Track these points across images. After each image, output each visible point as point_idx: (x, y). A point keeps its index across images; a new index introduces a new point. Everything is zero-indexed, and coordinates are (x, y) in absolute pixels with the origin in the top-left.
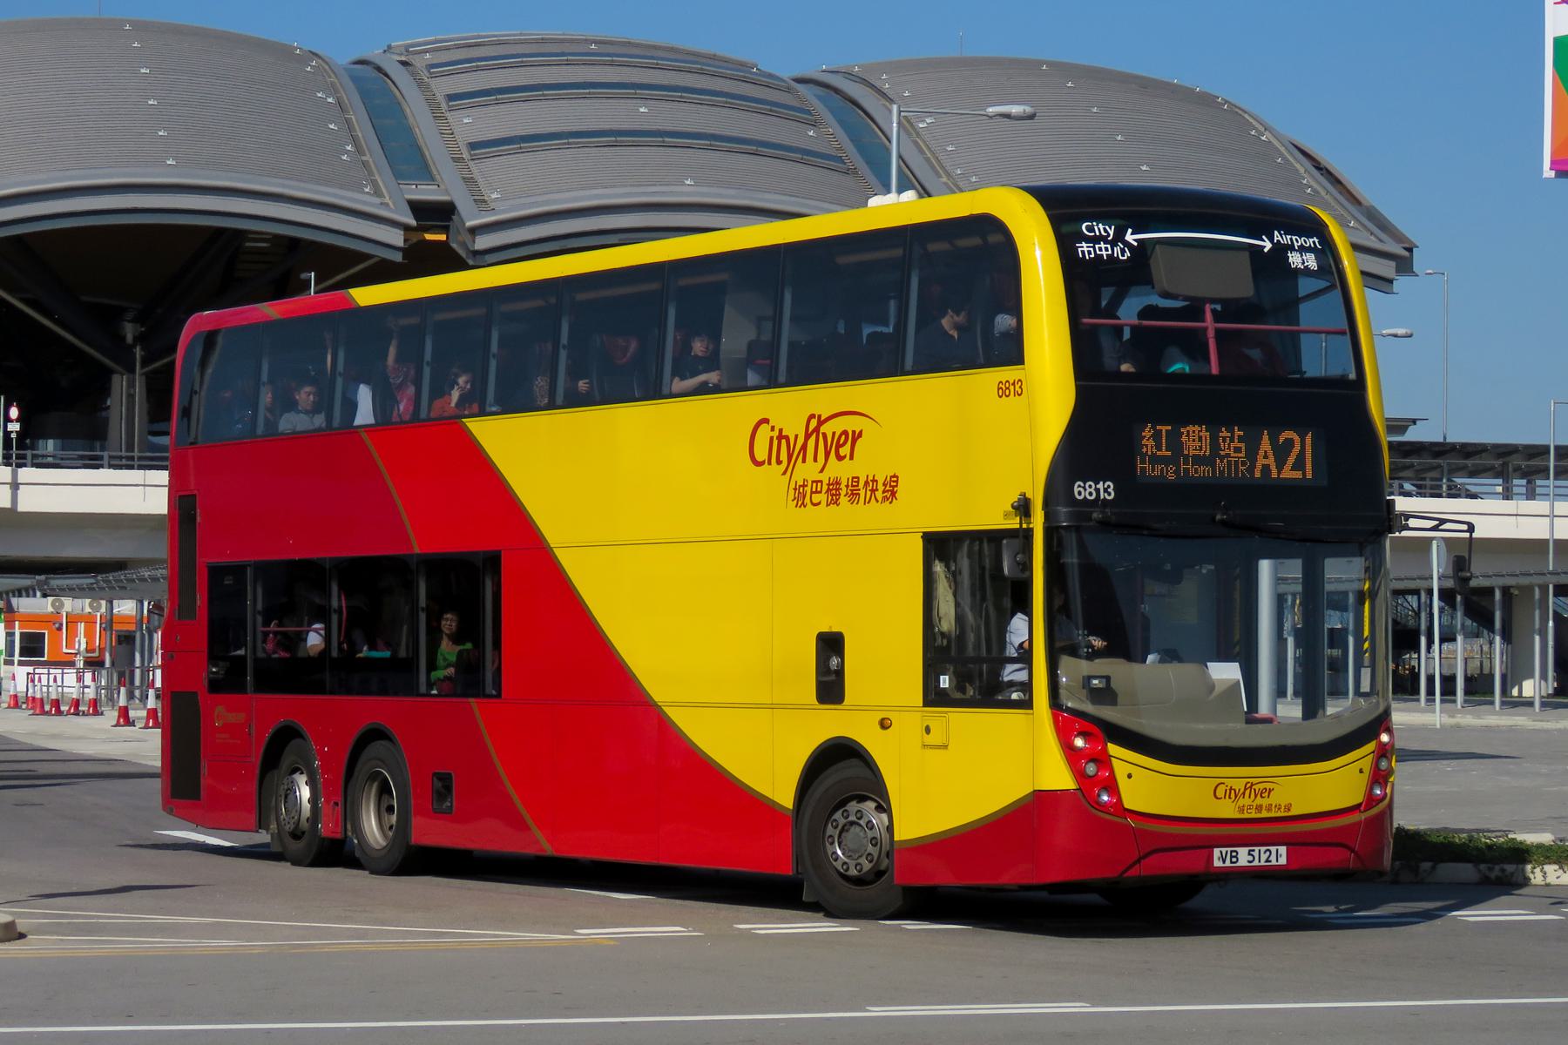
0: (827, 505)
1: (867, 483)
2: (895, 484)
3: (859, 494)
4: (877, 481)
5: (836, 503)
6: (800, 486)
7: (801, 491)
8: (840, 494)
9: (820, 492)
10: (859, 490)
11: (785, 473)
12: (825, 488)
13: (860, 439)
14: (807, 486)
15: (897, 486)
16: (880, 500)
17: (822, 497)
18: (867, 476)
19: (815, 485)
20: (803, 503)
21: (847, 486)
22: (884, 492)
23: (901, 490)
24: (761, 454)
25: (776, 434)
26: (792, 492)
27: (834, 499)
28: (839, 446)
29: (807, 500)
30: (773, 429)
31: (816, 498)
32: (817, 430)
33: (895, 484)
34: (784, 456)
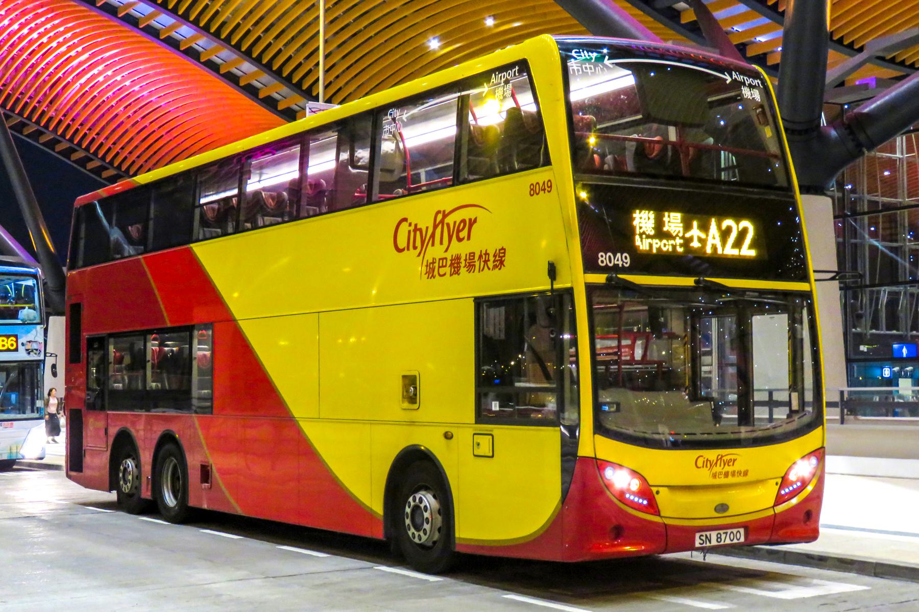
0: (451, 275)
1: (480, 256)
2: (503, 255)
3: (475, 265)
4: (488, 254)
5: (457, 273)
6: (430, 264)
7: (431, 265)
8: (460, 267)
9: (446, 266)
10: (475, 262)
11: (419, 255)
12: (449, 263)
13: (475, 227)
14: (435, 263)
15: (504, 256)
16: (491, 267)
17: (447, 270)
18: (481, 251)
19: (441, 261)
20: (433, 275)
21: (466, 260)
22: (494, 261)
23: (508, 260)
24: (402, 242)
25: (412, 228)
26: (424, 268)
27: (456, 271)
28: (459, 231)
29: (436, 272)
30: (410, 225)
31: (442, 271)
32: (442, 222)
33: (501, 255)
34: (418, 244)
